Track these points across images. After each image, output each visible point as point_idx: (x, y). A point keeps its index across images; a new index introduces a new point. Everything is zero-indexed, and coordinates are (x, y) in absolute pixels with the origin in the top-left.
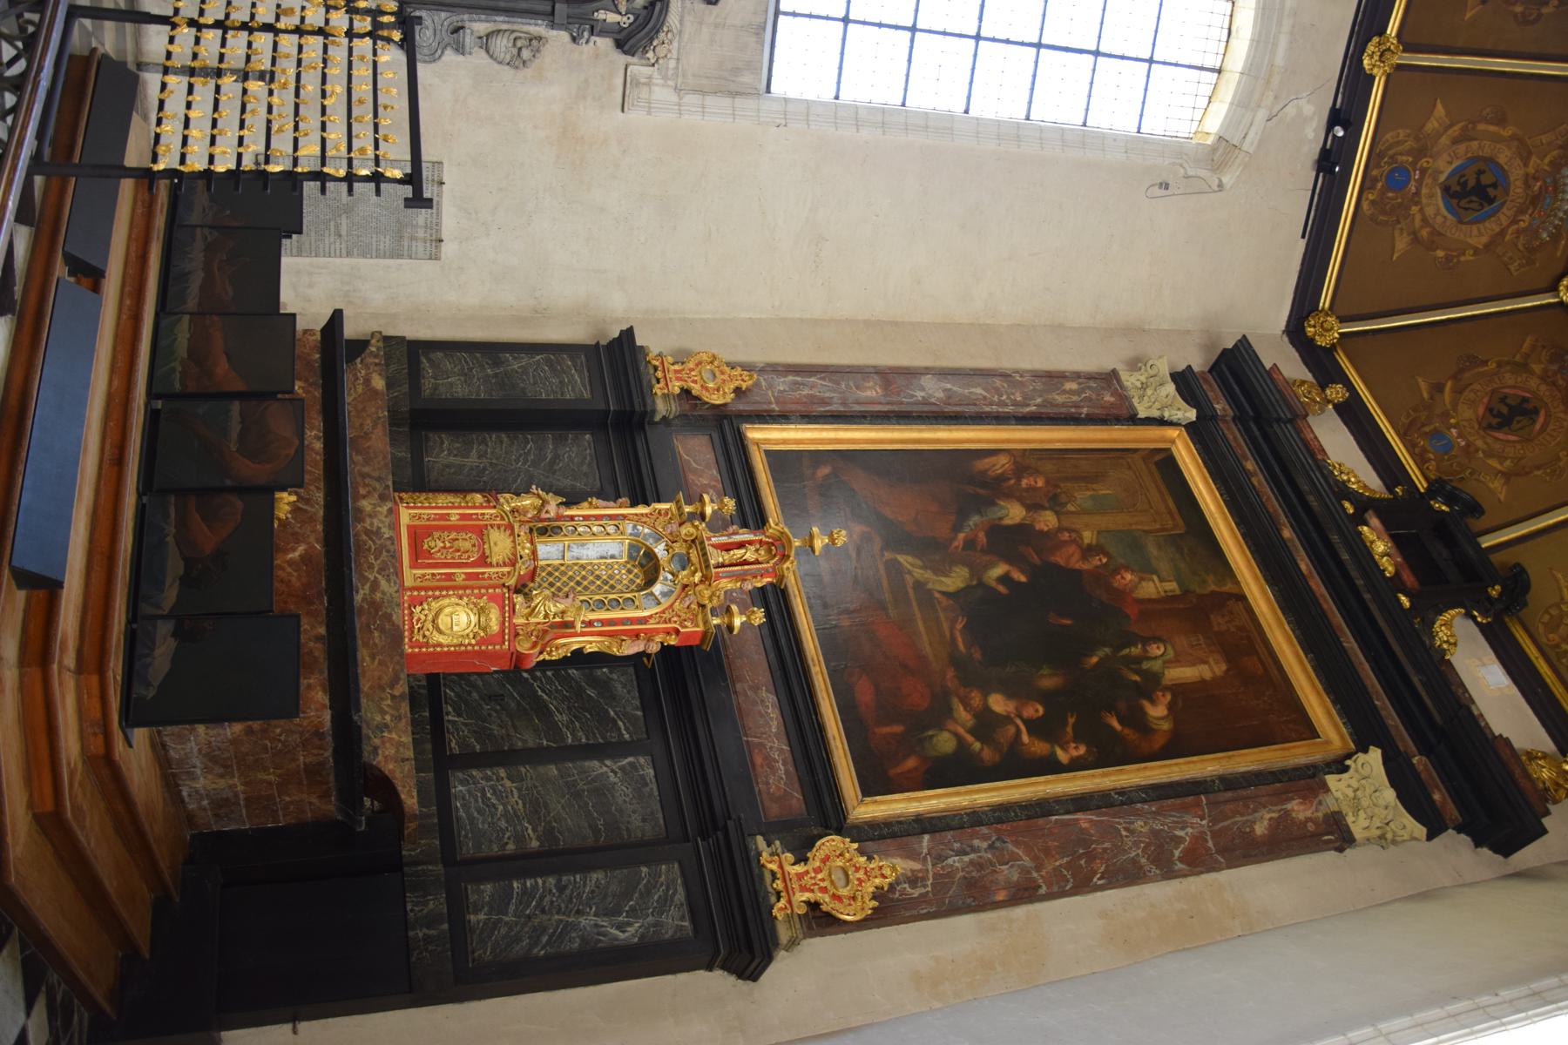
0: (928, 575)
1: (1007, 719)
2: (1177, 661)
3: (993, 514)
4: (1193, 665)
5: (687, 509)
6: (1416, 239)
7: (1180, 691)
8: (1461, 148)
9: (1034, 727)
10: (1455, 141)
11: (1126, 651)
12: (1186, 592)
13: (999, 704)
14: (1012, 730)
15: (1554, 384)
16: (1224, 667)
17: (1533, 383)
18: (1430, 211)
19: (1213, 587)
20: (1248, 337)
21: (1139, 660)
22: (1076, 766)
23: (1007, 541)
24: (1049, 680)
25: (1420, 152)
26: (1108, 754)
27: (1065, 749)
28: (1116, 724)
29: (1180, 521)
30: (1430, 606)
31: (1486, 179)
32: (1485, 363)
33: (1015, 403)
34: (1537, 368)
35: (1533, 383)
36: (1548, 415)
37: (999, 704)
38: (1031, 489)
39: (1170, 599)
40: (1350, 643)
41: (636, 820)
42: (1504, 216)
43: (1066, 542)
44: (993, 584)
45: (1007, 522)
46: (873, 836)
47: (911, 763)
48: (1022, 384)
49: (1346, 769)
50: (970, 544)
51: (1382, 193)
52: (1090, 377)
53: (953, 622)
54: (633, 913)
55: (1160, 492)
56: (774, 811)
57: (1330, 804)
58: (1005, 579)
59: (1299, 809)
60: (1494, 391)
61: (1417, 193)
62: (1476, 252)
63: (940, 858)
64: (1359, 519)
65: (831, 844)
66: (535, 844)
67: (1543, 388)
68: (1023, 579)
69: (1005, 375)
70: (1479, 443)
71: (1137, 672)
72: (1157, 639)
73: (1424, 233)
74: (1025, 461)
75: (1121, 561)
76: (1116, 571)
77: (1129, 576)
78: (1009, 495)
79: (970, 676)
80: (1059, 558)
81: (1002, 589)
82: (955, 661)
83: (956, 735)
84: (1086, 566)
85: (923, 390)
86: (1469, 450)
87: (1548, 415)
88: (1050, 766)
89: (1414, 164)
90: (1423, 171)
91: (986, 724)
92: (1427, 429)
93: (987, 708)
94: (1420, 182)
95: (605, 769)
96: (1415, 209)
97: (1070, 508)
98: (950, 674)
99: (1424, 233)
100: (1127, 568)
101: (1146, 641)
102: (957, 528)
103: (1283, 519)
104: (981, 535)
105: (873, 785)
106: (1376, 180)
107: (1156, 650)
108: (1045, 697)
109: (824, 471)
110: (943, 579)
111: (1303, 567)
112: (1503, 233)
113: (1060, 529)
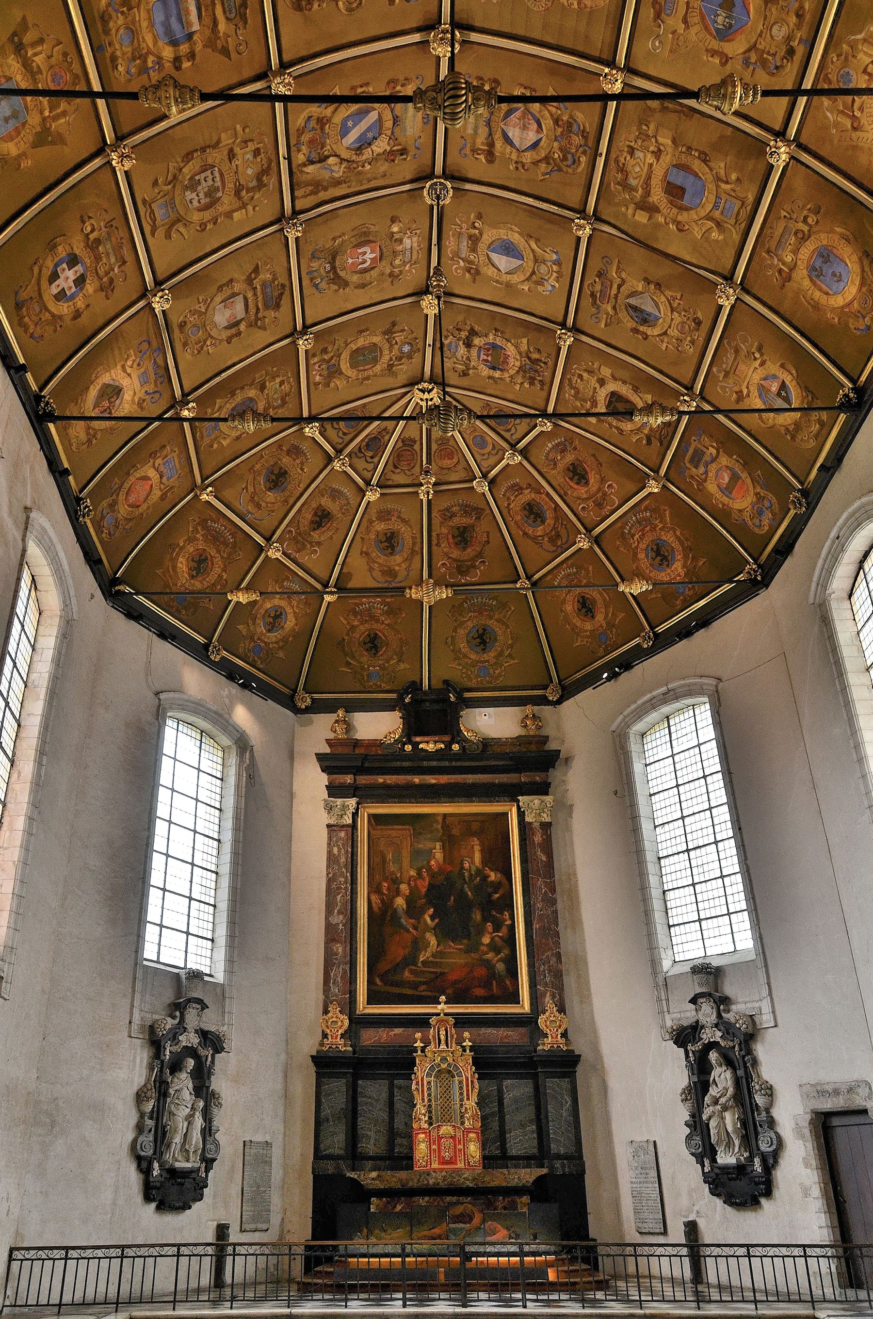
0: (429, 950)
1: (492, 939)
2: (472, 858)
3: (400, 911)
4: (474, 852)
5: (419, 1052)
6: (280, 648)
7: (485, 862)
8: (258, 621)
9: (497, 928)
10: (254, 624)
11: (467, 879)
12: (441, 840)
13: (486, 940)
14: (497, 938)
15: (366, 621)
16: (476, 839)
17: (362, 628)
18: (274, 639)
19: (439, 827)
20: (318, 752)
21: (471, 875)
22: (512, 918)
23: (413, 910)
24: (477, 916)
25: (252, 639)
26: (508, 904)
27: (506, 920)
28: (497, 895)
29: (407, 827)
30: (456, 735)
31: (272, 615)
32: (344, 639)
33: (346, 882)
34: (356, 623)
35: (362, 628)
36: (380, 631)
37: (486, 940)
38: (388, 889)
39: (443, 847)
40: (471, 778)
41: (527, 1090)
42: (289, 610)
43: (415, 885)
44: (434, 924)
45: (405, 906)
46: (537, 1006)
47: (508, 982)
48: (334, 875)
49: (524, 812)
50: (415, 928)
51: (260, 658)
52: (330, 838)
53: (450, 946)
54: (562, 1098)
55: (392, 829)
56: (526, 1040)
57: (537, 825)
58: (432, 918)
59: (538, 838)
60: (359, 643)
61: (266, 643)
62: (296, 624)
63: (546, 984)
64: (415, 745)
65: (541, 1021)
66: (534, 1127)
67: (366, 625)
68: (432, 910)
69: (329, 882)
70: (381, 662)
71: (475, 878)
72: (462, 863)
73: (281, 644)
74: (374, 888)
75: (425, 862)
76: (430, 867)
77: (433, 863)
78: (392, 901)
79: (473, 948)
80: (424, 890)
81: (437, 921)
82: (468, 951)
83: (498, 961)
84: (427, 879)
85: (338, 924)
86: (383, 668)
87: (380, 631)
88: (512, 928)
89: (255, 642)
90: (259, 639)
91: (494, 947)
92: (366, 678)
93: (487, 945)
94: (261, 640)
95: (508, 1098)
96: (271, 646)
97: (399, 875)
98: (473, 955)
99: (281, 644)
100: (429, 862)
101: (462, 868)
102: (408, 931)
103: (409, 777)
104: (412, 921)
105: (514, 998)
106: (254, 660)
107: (467, 865)
108: (485, 920)
109: (378, 981)
110: (432, 943)
111: (433, 781)
112: (295, 612)
113: (409, 884)
